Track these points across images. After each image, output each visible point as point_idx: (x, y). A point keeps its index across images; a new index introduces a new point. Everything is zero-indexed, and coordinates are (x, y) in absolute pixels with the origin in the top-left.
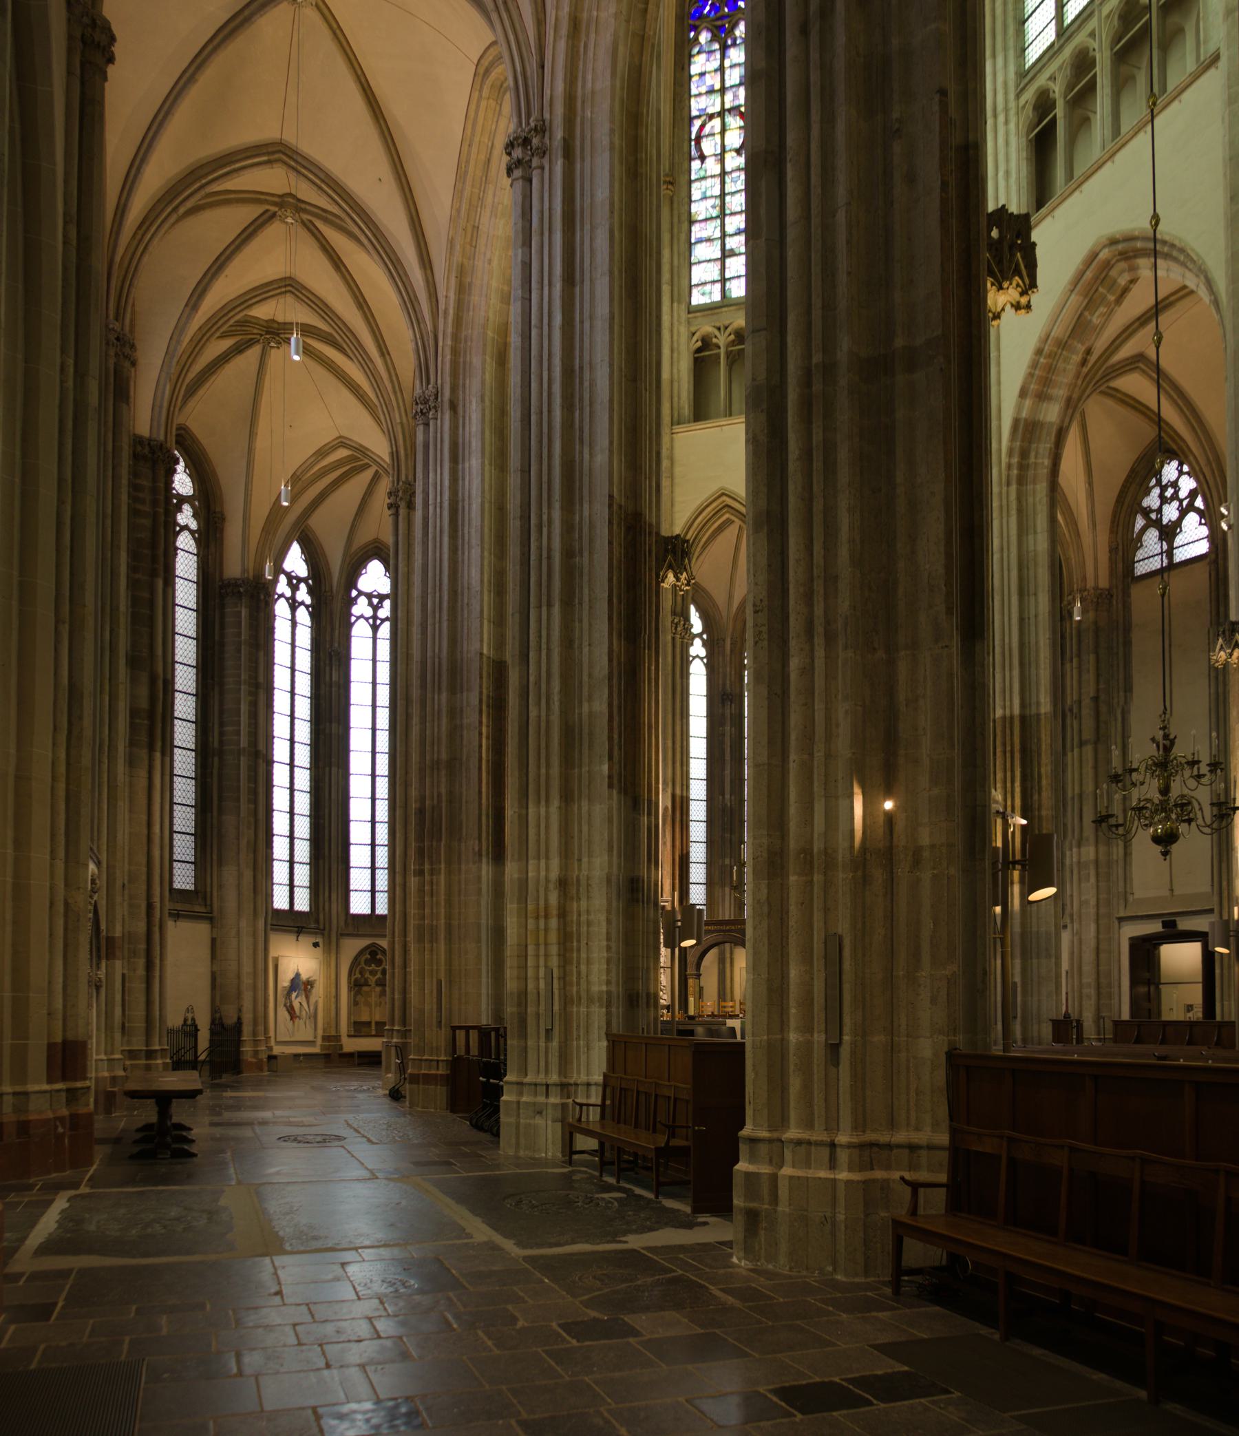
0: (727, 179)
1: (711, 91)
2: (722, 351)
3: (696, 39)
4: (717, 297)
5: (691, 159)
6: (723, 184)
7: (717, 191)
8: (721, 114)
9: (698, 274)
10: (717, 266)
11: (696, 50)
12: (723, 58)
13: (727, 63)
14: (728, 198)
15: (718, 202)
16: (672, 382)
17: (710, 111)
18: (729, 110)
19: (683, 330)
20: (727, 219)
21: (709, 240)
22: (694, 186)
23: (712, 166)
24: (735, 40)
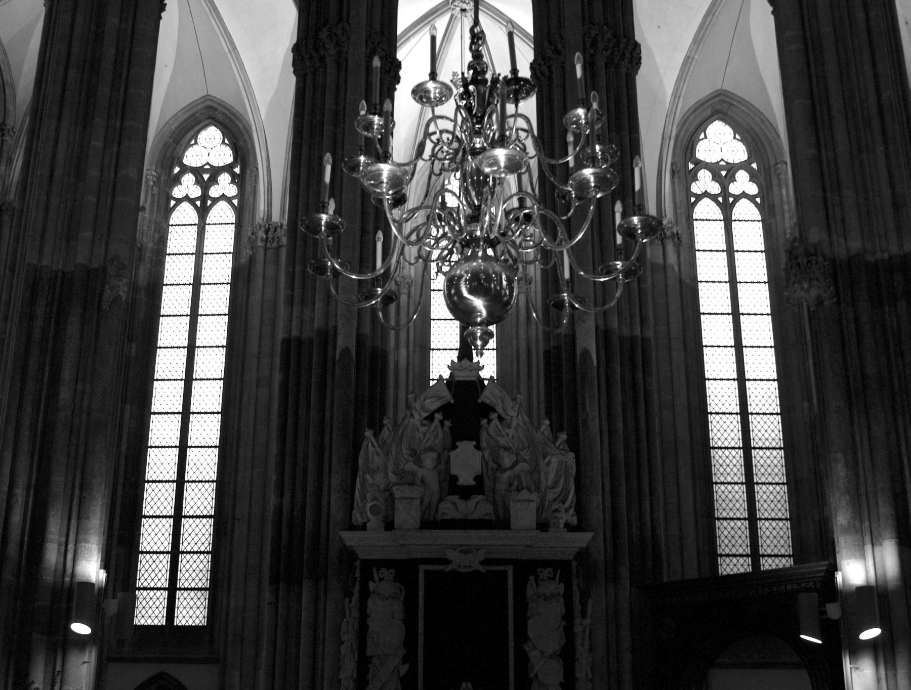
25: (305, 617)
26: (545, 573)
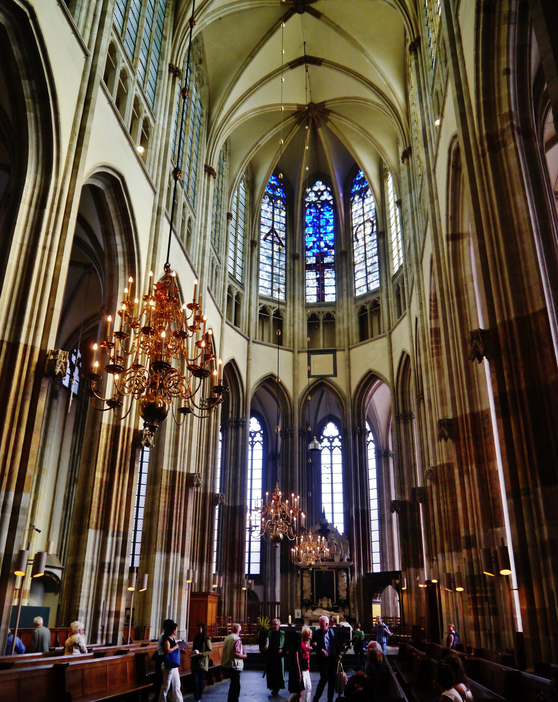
0: (367, 246)
1: (360, 216)
2: (368, 312)
3: (353, 200)
4: (365, 291)
5: (353, 242)
6: (365, 248)
7: (363, 251)
8: (363, 223)
9: (358, 284)
10: (364, 280)
11: (353, 204)
12: (363, 203)
13: (365, 204)
14: (367, 253)
15: (364, 255)
16: (348, 329)
17: (360, 223)
18: (366, 221)
19: (353, 307)
20: (367, 261)
21: (361, 270)
22: (355, 251)
23: (361, 243)
24: (367, 197)
25: (289, 581)
26: (342, 571)
